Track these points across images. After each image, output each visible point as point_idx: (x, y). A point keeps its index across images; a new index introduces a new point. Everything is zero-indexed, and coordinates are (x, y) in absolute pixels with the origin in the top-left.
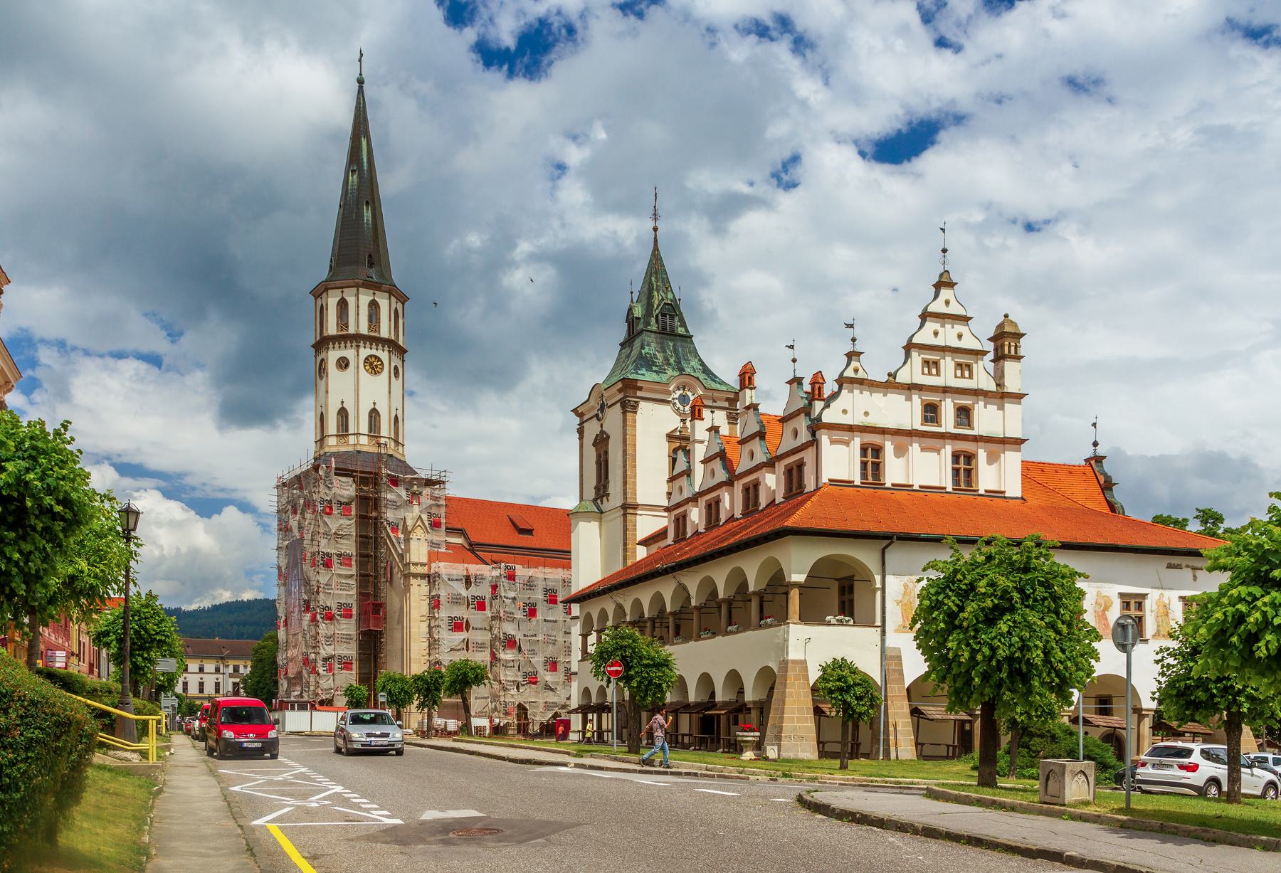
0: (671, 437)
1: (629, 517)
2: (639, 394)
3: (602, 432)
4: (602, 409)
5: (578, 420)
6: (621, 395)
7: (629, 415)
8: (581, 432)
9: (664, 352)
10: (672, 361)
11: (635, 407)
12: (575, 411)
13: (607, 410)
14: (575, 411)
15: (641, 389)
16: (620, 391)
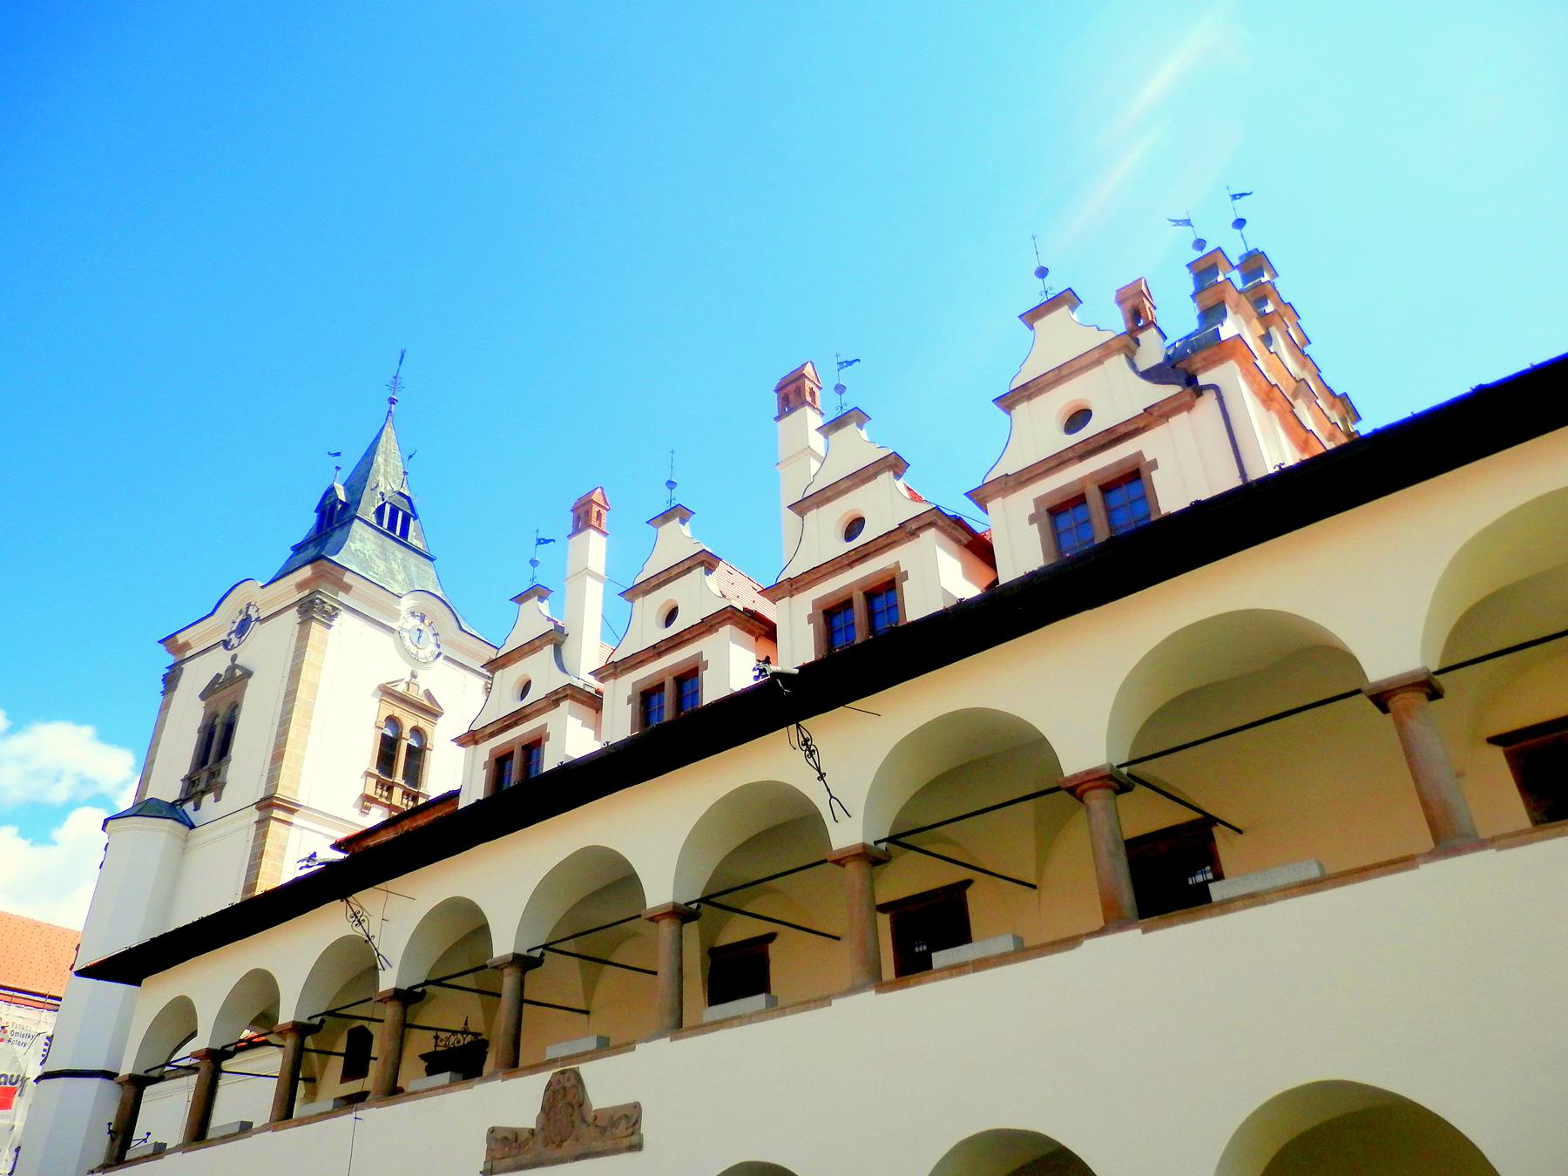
0: (388, 692)
1: (274, 826)
2: (342, 597)
3: (233, 667)
4: (243, 627)
5: (170, 660)
6: (307, 592)
7: (316, 629)
8: (171, 680)
9: (386, 560)
10: (400, 577)
11: (330, 616)
12: (168, 641)
13: (256, 630)
14: (168, 641)
15: (347, 588)
16: (300, 586)
